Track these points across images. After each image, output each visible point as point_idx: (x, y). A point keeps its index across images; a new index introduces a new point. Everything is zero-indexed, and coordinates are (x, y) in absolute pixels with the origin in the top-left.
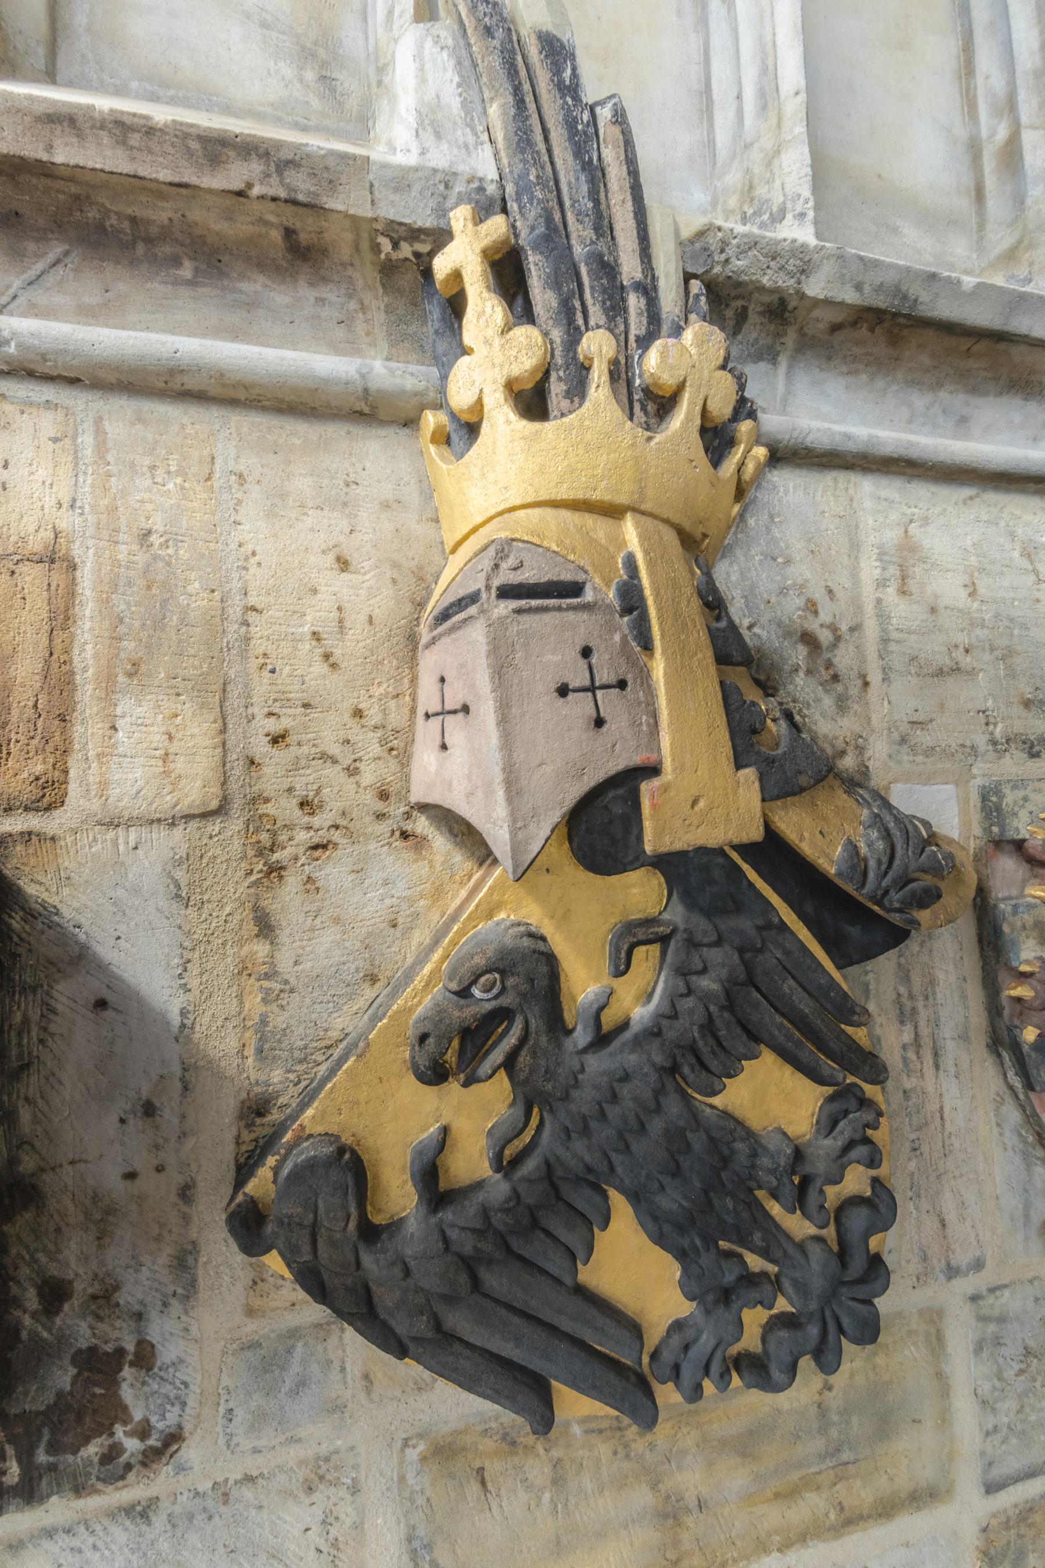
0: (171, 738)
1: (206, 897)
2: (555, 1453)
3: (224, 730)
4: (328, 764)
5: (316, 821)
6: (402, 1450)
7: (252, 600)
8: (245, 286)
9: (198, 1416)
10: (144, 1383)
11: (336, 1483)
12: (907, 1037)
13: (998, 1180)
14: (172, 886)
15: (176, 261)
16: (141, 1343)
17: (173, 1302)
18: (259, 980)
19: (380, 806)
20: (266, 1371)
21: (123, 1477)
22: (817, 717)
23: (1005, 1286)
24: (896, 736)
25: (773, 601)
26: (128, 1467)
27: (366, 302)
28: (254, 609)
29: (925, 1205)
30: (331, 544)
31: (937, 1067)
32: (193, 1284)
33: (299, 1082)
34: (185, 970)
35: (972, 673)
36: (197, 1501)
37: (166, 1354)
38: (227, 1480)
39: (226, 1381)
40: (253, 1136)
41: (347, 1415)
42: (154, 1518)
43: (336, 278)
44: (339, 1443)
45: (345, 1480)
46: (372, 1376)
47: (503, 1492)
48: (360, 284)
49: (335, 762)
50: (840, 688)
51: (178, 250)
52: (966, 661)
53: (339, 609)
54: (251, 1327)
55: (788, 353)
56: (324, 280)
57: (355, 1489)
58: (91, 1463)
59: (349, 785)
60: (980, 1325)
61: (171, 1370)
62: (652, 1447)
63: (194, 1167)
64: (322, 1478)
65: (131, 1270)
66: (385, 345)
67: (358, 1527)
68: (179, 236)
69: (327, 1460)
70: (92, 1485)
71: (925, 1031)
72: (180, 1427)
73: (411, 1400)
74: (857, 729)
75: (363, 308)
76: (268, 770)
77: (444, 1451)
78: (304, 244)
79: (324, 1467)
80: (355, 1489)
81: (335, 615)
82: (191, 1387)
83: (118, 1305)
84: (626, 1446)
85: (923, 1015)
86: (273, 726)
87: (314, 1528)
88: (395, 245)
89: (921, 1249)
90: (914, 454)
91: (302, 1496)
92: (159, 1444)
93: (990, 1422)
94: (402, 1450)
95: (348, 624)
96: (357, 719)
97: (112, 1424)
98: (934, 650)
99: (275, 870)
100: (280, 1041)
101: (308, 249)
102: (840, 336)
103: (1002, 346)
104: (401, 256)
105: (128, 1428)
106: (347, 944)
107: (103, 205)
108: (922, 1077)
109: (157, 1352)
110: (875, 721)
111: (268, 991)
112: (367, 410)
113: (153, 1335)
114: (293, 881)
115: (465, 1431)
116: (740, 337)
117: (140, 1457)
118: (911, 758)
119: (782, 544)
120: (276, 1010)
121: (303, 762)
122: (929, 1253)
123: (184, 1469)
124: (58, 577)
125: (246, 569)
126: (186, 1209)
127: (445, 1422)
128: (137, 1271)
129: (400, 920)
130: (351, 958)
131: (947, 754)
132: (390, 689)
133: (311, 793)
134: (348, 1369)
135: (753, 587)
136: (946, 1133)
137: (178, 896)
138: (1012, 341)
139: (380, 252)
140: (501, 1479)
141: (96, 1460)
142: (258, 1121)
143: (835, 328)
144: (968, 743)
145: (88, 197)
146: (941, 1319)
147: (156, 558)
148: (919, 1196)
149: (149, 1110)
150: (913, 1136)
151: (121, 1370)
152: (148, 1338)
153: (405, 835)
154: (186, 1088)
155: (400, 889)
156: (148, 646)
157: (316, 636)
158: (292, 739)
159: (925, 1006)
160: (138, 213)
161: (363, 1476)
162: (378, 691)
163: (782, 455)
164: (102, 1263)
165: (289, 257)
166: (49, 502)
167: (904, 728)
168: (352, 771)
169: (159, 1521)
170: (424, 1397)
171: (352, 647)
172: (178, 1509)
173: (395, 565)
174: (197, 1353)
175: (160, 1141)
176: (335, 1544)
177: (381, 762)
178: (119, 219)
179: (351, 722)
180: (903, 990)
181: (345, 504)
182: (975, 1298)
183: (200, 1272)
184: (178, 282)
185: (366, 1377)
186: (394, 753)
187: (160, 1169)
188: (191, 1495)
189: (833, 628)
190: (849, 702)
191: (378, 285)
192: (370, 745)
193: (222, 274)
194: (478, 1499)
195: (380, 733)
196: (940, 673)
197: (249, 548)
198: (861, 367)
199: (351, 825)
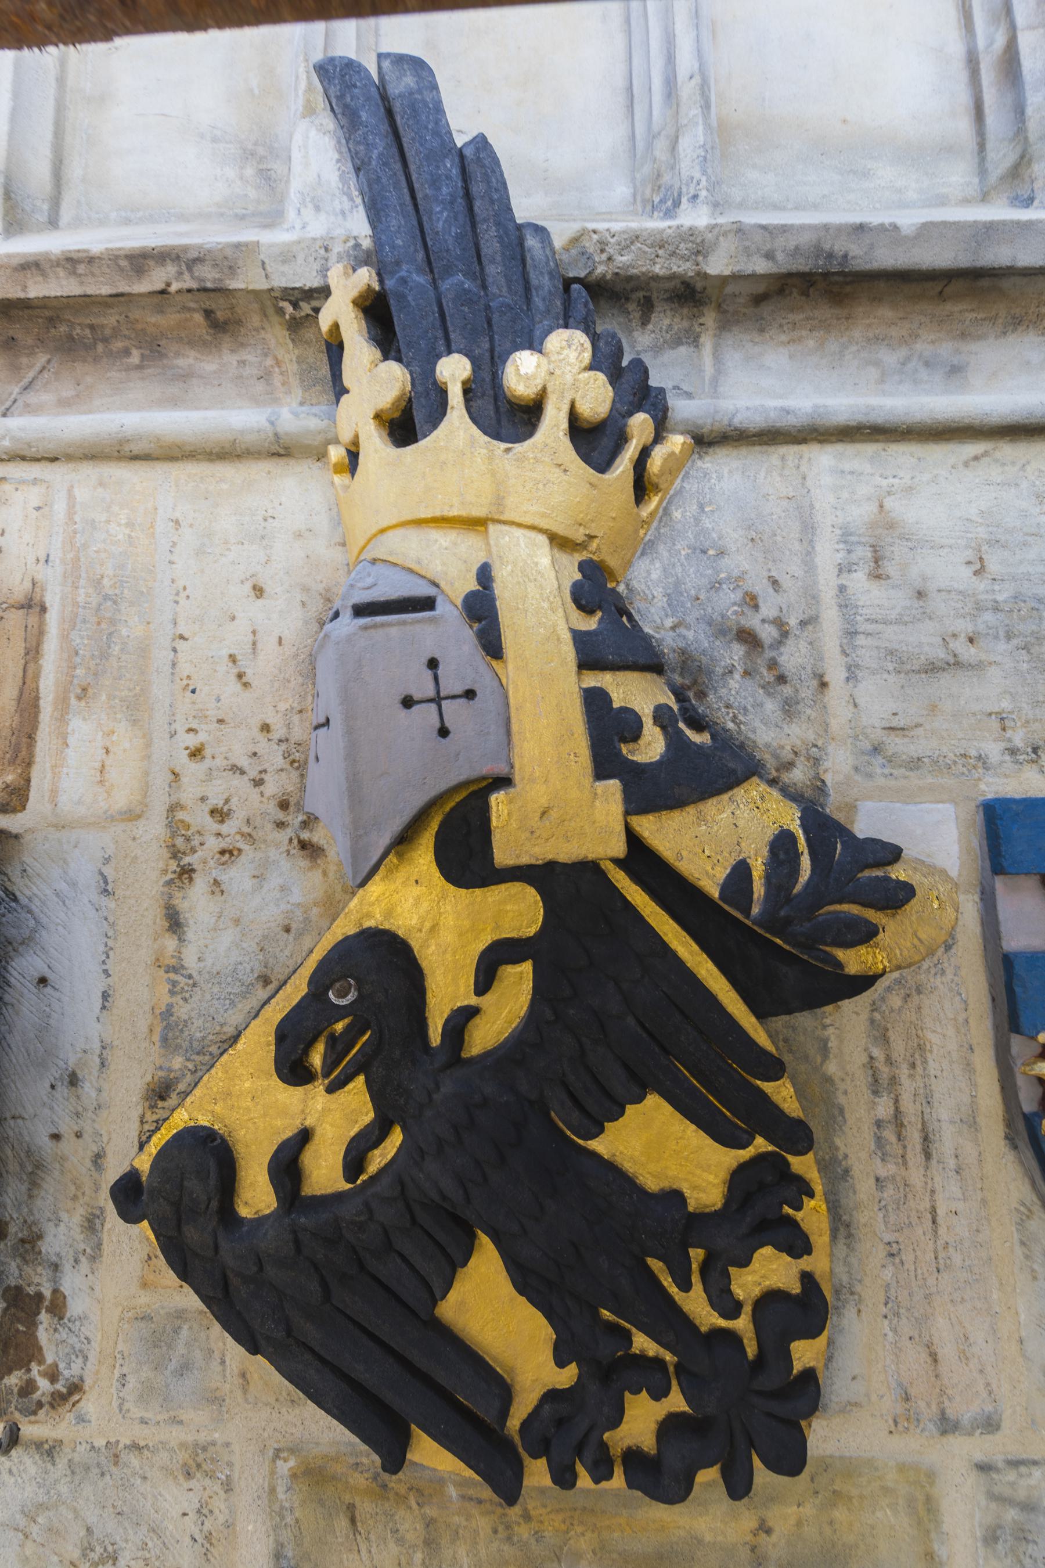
0: (107, 752)
1: (128, 893)
2: (430, 1511)
3: (148, 745)
4: (237, 775)
5: (224, 829)
6: (274, 1461)
7: (182, 629)
8: (180, 362)
9: (97, 1372)
10: (56, 1330)
11: (211, 1475)
12: (884, 1108)
13: (1023, 1317)
14: (101, 881)
15: (127, 352)
16: (55, 1291)
17: (83, 1259)
18: (167, 972)
19: (281, 816)
20: (155, 1346)
21: (35, 1413)
22: (757, 723)
23: (1035, 1463)
24: (867, 746)
25: (702, 597)
26: (40, 1405)
27: (280, 357)
28: (182, 637)
29: (906, 1328)
30: (248, 574)
31: (928, 1156)
32: (99, 1245)
33: (196, 1071)
34: (108, 957)
35: (978, 667)
36: (92, 1454)
37: (75, 1307)
38: (118, 1442)
39: (121, 1346)
40: (155, 1117)
41: (224, 1409)
42: (58, 1460)
43: (252, 342)
44: (217, 1435)
45: (219, 1475)
46: (248, 1376)
47: (372, 1537)
48: (272, 343)
49: (243, 773)
50: (787, 690)
51: (127, 343)
52: (968, 653)
53: (254, 632)
54: (144, 1299)
55: (711, 332)
56: (242, 345)
57: (228, 1487)
58: (12, 1393)
59: (254, 793)
60: (993, 1506)
61: (77, 1323)
62: (539, 1537)
63: (105, 1139)
64: (199, 1466)
65: (51, 1224)
66: (298, 393)
67: (229, 1525)
68: (127, 333)
69: (204, 1449)
70: (12, 1413)
71: (908, 1106)
72: (82, 1379)
73: (284, 1410)
74: (811, 736)
75: (278, 363)
76: (184, 780)
77: (314, 1475)
78: (222, 319)
79: (202, 1456)
80: (228, 1487)
81: (250, 637)
82: (93, 1343)
83: (40, 1253)
84: (508, 1527)
85: (907, 1087)
86: (192, 741)
87: (191, 1515)
88: (295, 305)
89: (900, 1385)
90: (878, 418)
91: (181, 1478)
92: (64, 1390)
94: (274, 1461)
95: (259, 646)
96: (265, 733)
97: (30, 1361)
98: (924, 641)
99: (187, 873)
100: (182, 1031)
101: (226, 323)
102: (766, 309)
103: (985, 283)
104: (303, 314)
105: (42, 1368)
106: (245, 945)
107: (69, 321)
108: (905, 1163)
109: (68, 1303)
110: (835, 725)
111: (174, 984)
112: (282, 452)
113: (66, 1288)
114: (200, 885)
115: (336, 1459)
116: (650, 327)
117: (49, 1399)
118: (887, 771)
119: (714, 535)
120: (181, 1002)
121: (215, 773)
122: (913, 1392)
123: (83, 1421)
125: (177, 602)
126: (95, 1175)
127: (317, 1444)
128: (56, 1225)
129: (294, 926)
130: (247, 959)
131: (938, 765)
132: (295, 705)
133: (221, 802)
134: (227, 1363)
135: (678, 583)
136: (940, 1243)
137: (106, 890)
138: (995, 275)
139: (284, 314)
140: (371, 1522)
141: (16, 1390)
142: (160, 1104)
143: (759, 300)
144: (973, 753)
145: (58, 317)
146: (932, 1484)
147: (106, 597)
148: (897, 1315)
149: (73, 1080)
150: (888, 1237)
151: (39, 1313)
152: (62, 1289)
153: (304, 845)
154: (103, 1065)
155: (296, 897)
156: (95, 674)
157: (233, 659)
158: (208, 752)
159: (911, 1076)
160: (94, 322)
161: (236, 1476)
162: (283, 706)
163: (704, 441)
164: (31, 1212)
165: (212, 331)
166: (31, 560)
167: (878, 735)
168: (258, 783)
169: (62, 1463)
170: (297, 1411)
171: (263, 668)
172: (77, 1458)
173: (306, 589)
174: (99, 1313)
175: (80, 1109)
176: (208, 1537)
177: (283, 774)
178: (82, 329)
179: (261, 738)
180: (876, 1052)
181: (263, 537)
182: (984, 1468)
183: (105, 1237)
184: (128, 369)
185: (243, 1375)
186: (296, 765)
187: (79, 1135)
188: (88, 1447)
189: (779, 623)
190: (799, 707)
191: (289, 341)
192: (274, 758)
194: (347, 1537)
195: (284, 746)
196: (932, 668)
197: (180, 584)
198: (804, 333)
199: (254, 834)
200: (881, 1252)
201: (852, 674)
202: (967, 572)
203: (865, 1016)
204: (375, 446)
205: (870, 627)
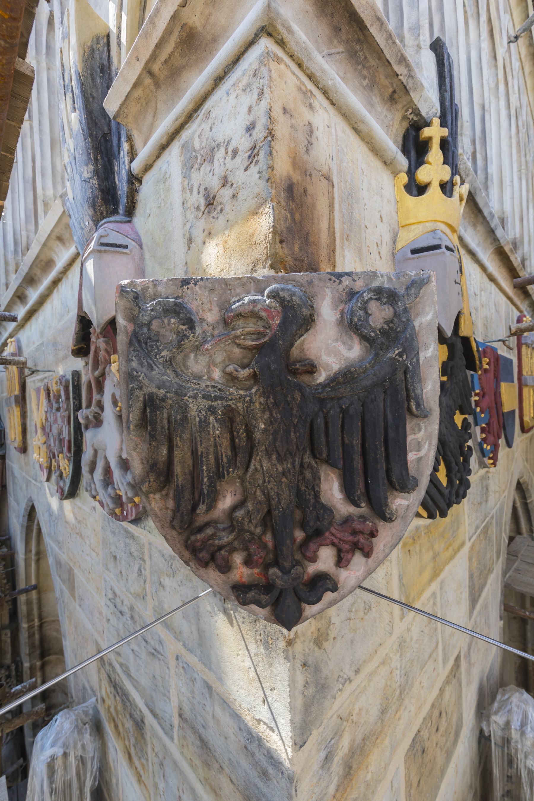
8: (374, 98)
15: (365, 78)
51: (367, 75)
80: (391, 562)
124: (330, 189)
193: (372, 90)
204: (435, 191)
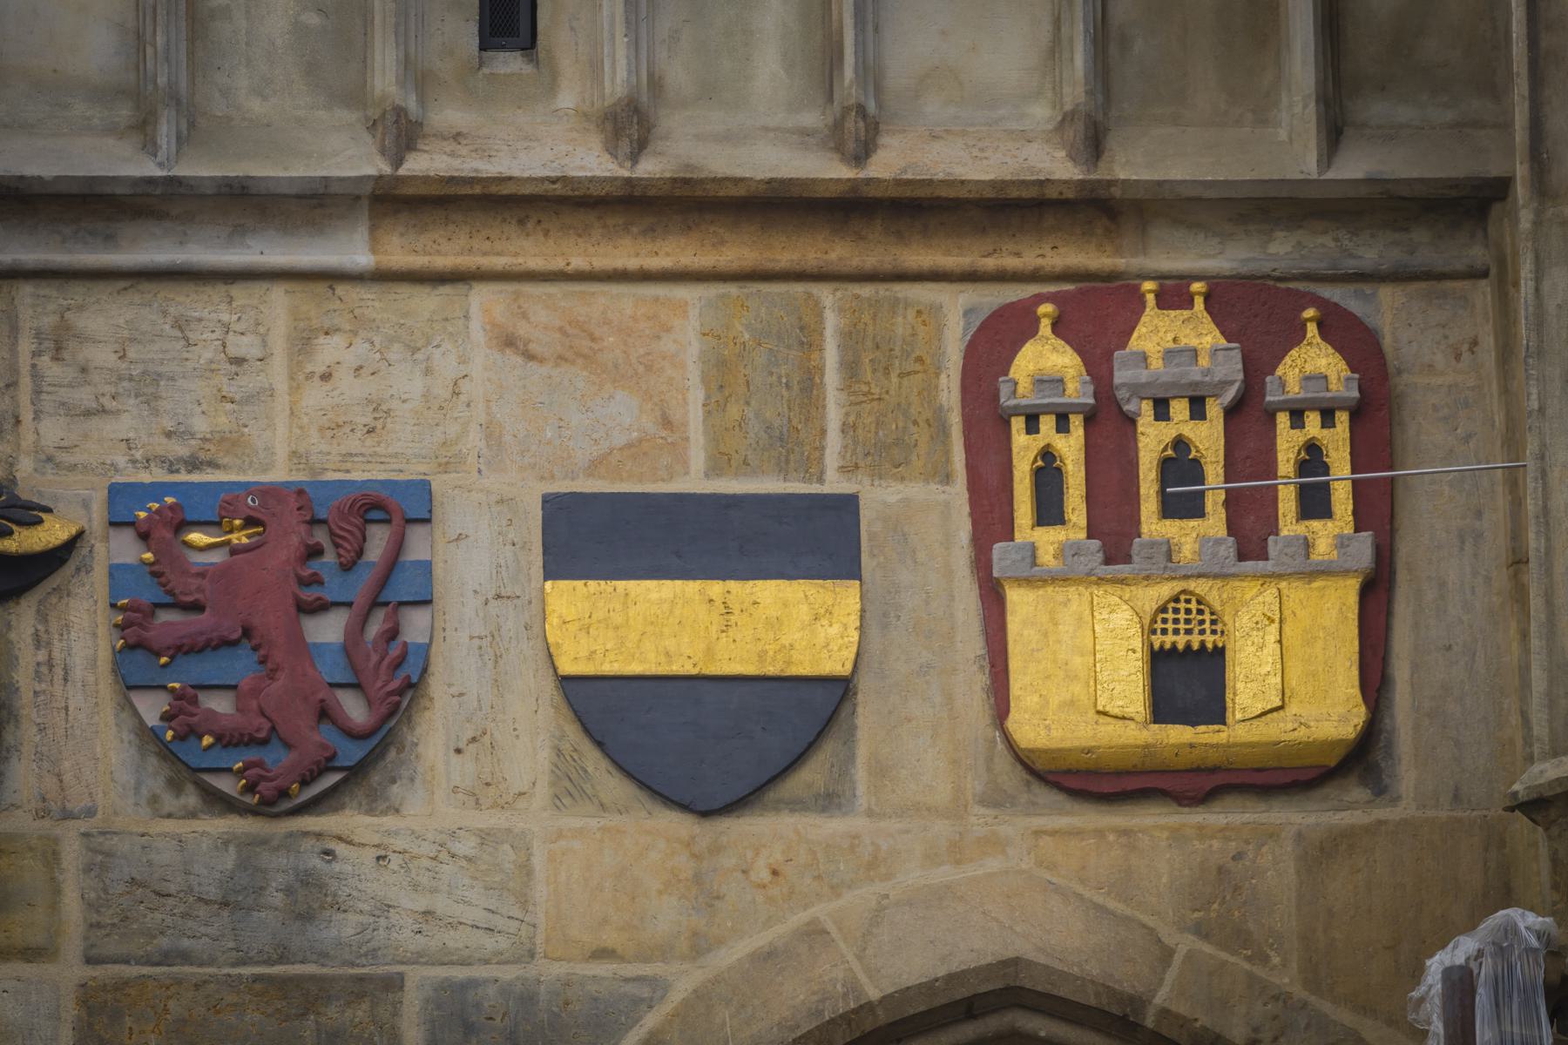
12: (42, 656)
31: (66, 680)
71: (56, 654)
93: (95, 918)
110: (24, 444)
182: (86, 835)
200: (35, 729)
201: (37, 416)
202: (114, 357)
203: (34, 609)
205: (50, 389)
